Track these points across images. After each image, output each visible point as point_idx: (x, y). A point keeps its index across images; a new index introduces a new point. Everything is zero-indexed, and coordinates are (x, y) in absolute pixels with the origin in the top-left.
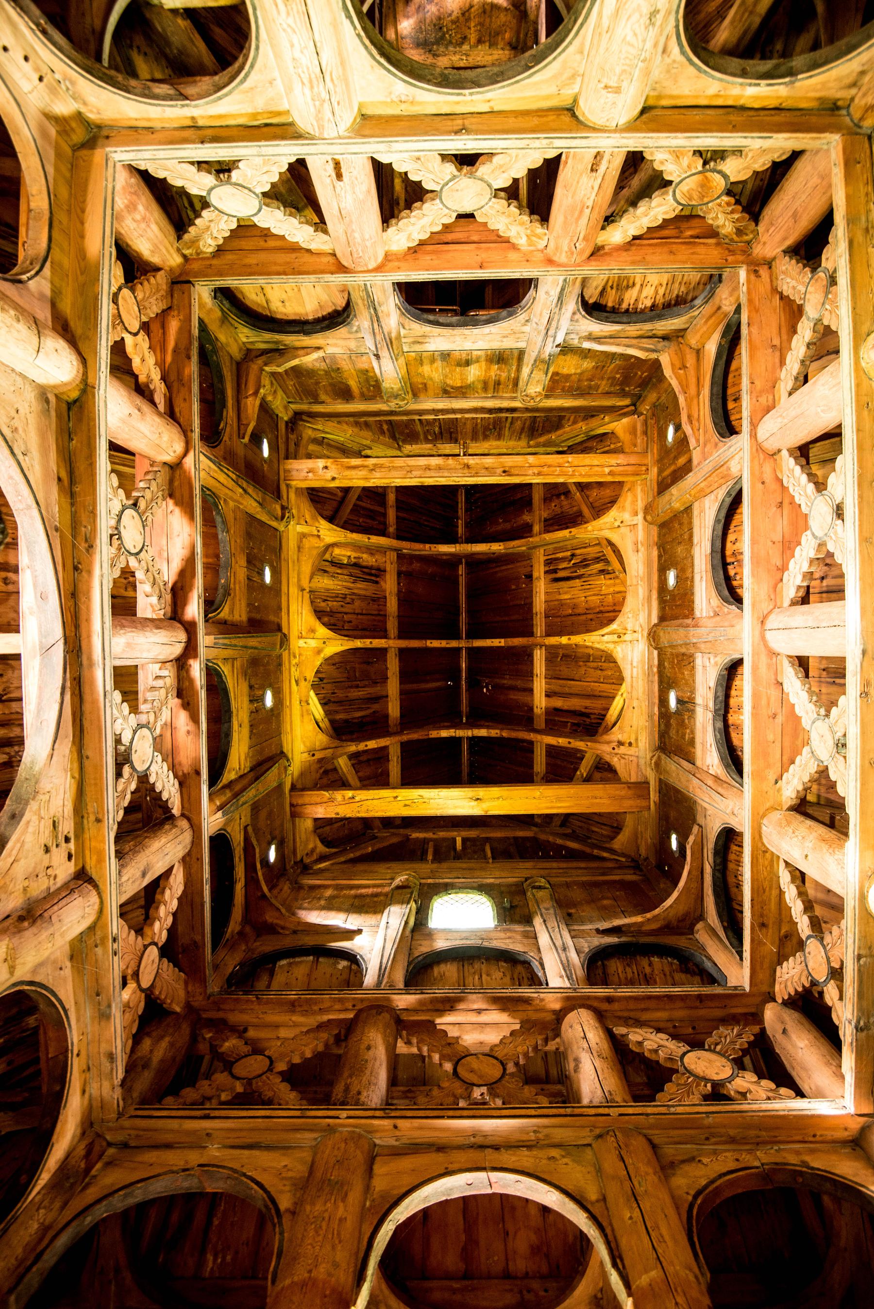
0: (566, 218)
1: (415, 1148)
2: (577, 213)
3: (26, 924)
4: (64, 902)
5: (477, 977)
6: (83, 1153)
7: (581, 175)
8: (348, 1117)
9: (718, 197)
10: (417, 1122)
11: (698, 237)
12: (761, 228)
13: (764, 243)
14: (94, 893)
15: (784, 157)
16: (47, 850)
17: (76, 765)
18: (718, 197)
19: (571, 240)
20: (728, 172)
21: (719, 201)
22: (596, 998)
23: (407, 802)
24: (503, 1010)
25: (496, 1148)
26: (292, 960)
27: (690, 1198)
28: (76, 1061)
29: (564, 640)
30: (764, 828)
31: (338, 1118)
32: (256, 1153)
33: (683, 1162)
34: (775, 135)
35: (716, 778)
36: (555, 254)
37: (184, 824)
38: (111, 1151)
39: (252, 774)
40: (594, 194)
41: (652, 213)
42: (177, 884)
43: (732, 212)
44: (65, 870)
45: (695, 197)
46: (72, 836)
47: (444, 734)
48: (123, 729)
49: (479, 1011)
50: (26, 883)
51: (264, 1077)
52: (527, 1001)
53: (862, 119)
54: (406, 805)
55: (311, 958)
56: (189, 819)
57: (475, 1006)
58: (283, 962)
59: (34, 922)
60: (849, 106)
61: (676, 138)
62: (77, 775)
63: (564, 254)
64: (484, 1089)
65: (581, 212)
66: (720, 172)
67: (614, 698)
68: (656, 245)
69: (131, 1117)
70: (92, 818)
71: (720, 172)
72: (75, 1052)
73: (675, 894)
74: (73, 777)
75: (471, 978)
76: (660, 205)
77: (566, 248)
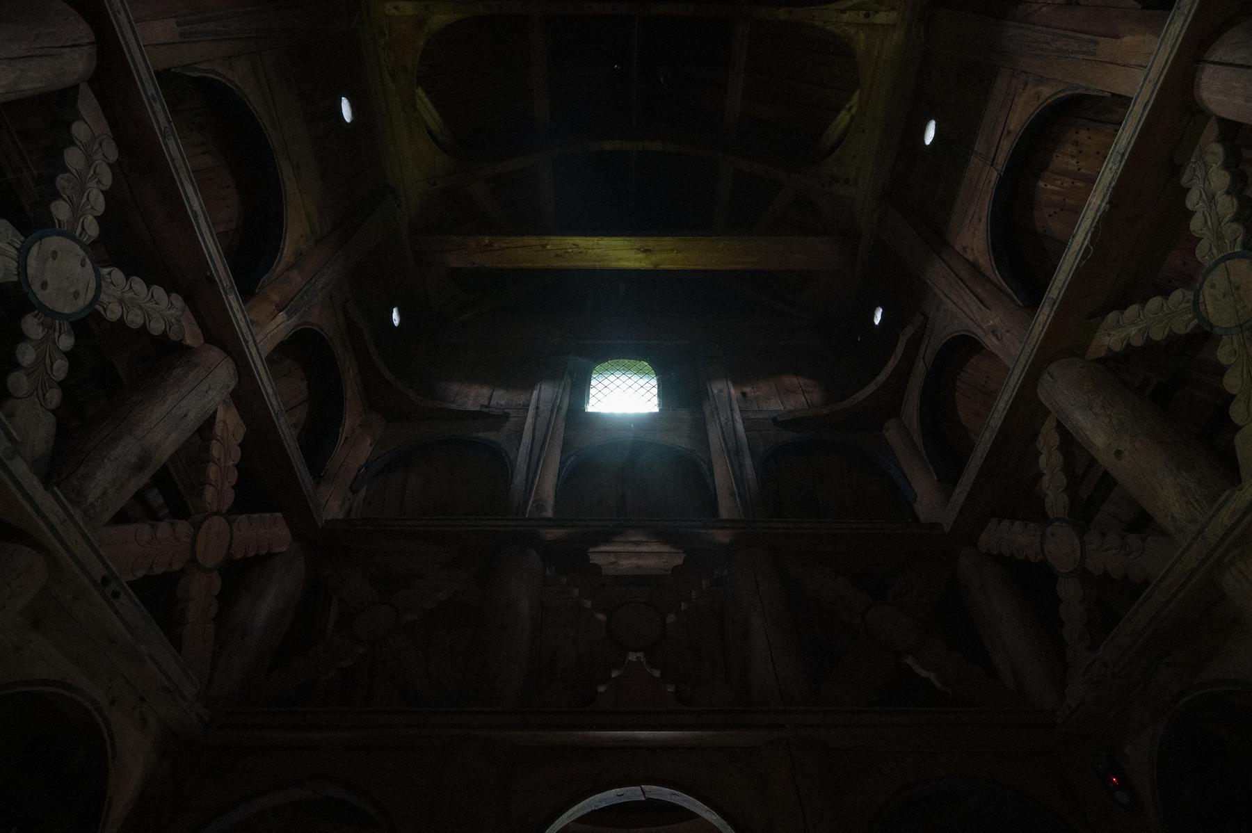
23: (560, 252)
29: (782, 14)
30: (1047, 377)
35: (974, 266)
37: (215, 353)
47: (608, 146)
49: (637, 543)
54: (557, 256)
56: (223, 347)
67: (838, 111)
73: (871, 388)
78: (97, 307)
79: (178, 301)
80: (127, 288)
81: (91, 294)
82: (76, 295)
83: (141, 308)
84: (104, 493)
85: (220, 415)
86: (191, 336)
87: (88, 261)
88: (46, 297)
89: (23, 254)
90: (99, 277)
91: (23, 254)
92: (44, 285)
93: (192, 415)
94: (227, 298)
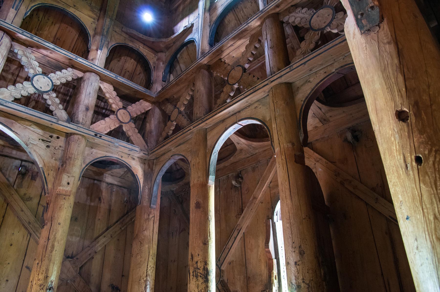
1: (216, 125)
3: (64, 166)
4: (69, 149)
5: (242, 12)
6: (148, 167)
8: (193, 128)
10: (211, 119)
14: (75, 136)
16: (48, 146)
17: (27, 123)
22: (271, 10)
24: (240, 39)
25: (239, 112)
26: (180, 53)
27: (302, 102)
28: (123, 159)
31: (191, 129)
32: (181, 146)
33: (302, 85)
37: (88, 74)
38: (155, 161)
39: (102, 13)
42: (108, 89)
44: (61, 142)
46: (51, 134)
48: (27, 92)
50: (54, 158)
51: (178, 117)
52: (246, 30)
55: (185, 47)
57: (229, 45)
58: (178, 56)
59: (66, 163)
62: (30, 124)
64: (237, 84)
69: (151, 154)
70: (50, 125)
72: (120, 158)
74: (30, 126)
75: (240, 14)
78: (54, 84)
79: (70, 69)
80: (57, 76)
81: (51, 83)
82: (48, 85)
83: (63, 77)
84: (83, 119)
85: (102, 87)
86: (80, 74)
87: (44, 77)
88: (43, 89)
89: (32, 84)
90: (49, 78)
91: (32, 84)
92: (41, 88)
93: (91, 92)
94: (77, 60)
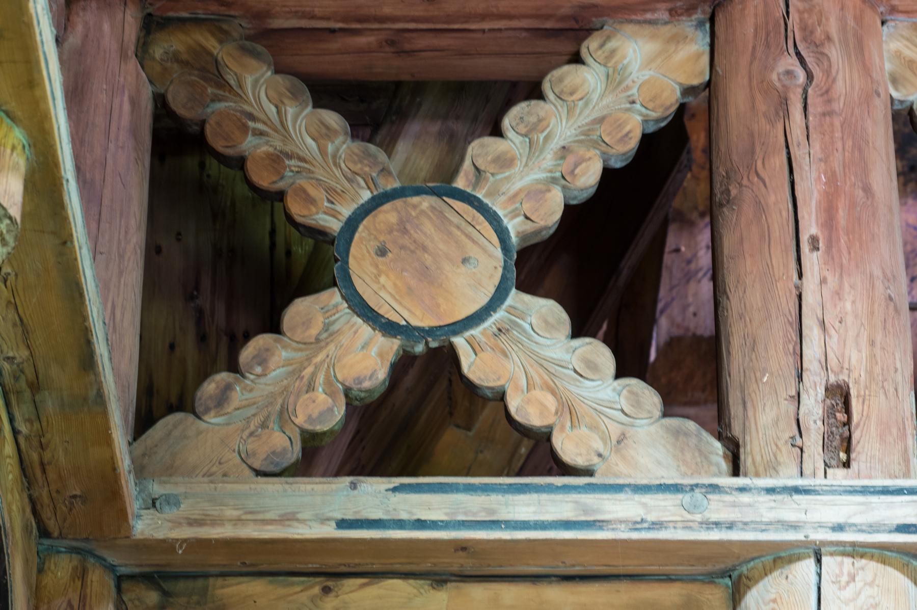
0: (867, 190)
2: (842, 215)
7: (870, 373)
9: (352, 224)
11: (332, 31)
12: (147, 92)
13: (123, 55)
15: (210, 387)
18: (352, 224)
19: (827, 93)
20: (366, 330)
21: (346, 211)
34: (329, 531)
36: (859, 20)
40: (810, 300)
41: (548, 159)
43: (276, 160)
45: (428, 227)
53: (81, 574)
60: (119, 590)
61: (636, 525)
63: (833, 28)
65: (829, 221)
66: (389, 328)
68: (484, 17)
71: (389, 328)
76: (536, 193)
77: (834, 53)
